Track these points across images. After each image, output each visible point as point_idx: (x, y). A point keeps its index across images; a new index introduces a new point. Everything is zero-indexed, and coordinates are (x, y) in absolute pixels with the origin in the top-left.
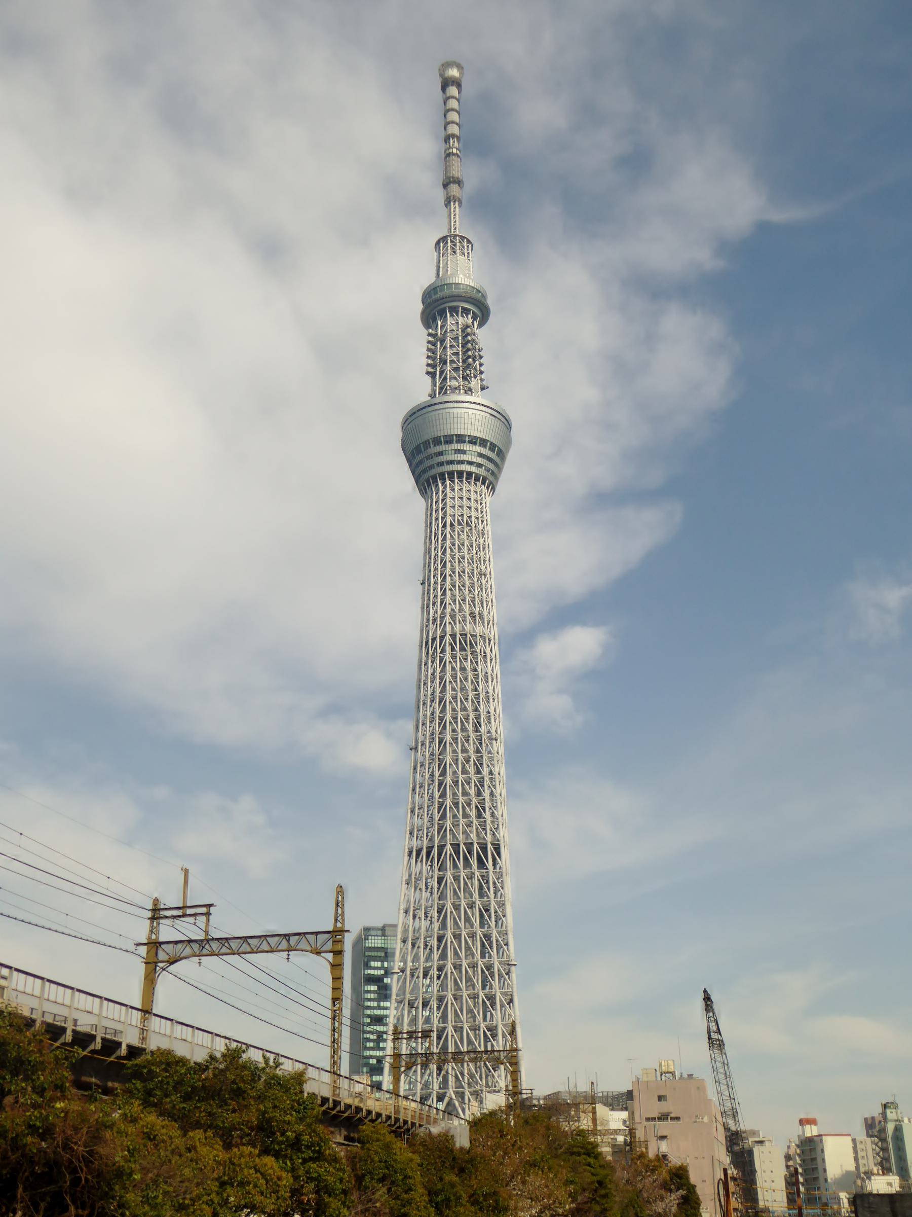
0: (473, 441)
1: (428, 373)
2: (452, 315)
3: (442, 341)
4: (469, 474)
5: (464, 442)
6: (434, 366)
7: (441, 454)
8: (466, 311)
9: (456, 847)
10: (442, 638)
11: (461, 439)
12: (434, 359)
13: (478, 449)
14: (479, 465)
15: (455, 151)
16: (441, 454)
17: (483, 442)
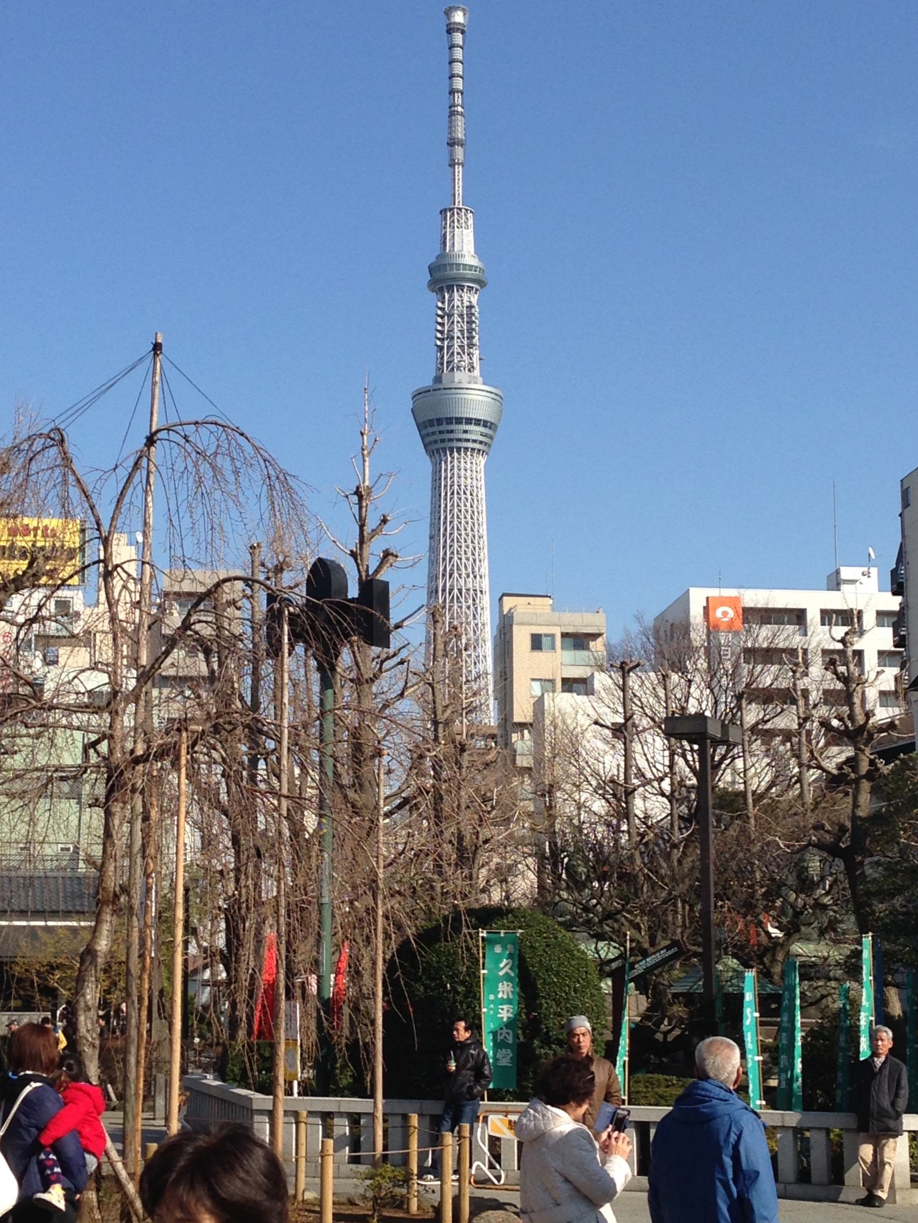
0: (478, 422)
2: (458, 291)
3: (450, 316)
4: (473, 449)
6: (442, 340)
7: (452, 431)
8: (470, 289)
10: (451, 590)
11: (469, 421)
12: (442, 332)
13: (481, 429)
14: (481, 442)
15: (460, 109)
16: (452, 431)
17: (485, 424)
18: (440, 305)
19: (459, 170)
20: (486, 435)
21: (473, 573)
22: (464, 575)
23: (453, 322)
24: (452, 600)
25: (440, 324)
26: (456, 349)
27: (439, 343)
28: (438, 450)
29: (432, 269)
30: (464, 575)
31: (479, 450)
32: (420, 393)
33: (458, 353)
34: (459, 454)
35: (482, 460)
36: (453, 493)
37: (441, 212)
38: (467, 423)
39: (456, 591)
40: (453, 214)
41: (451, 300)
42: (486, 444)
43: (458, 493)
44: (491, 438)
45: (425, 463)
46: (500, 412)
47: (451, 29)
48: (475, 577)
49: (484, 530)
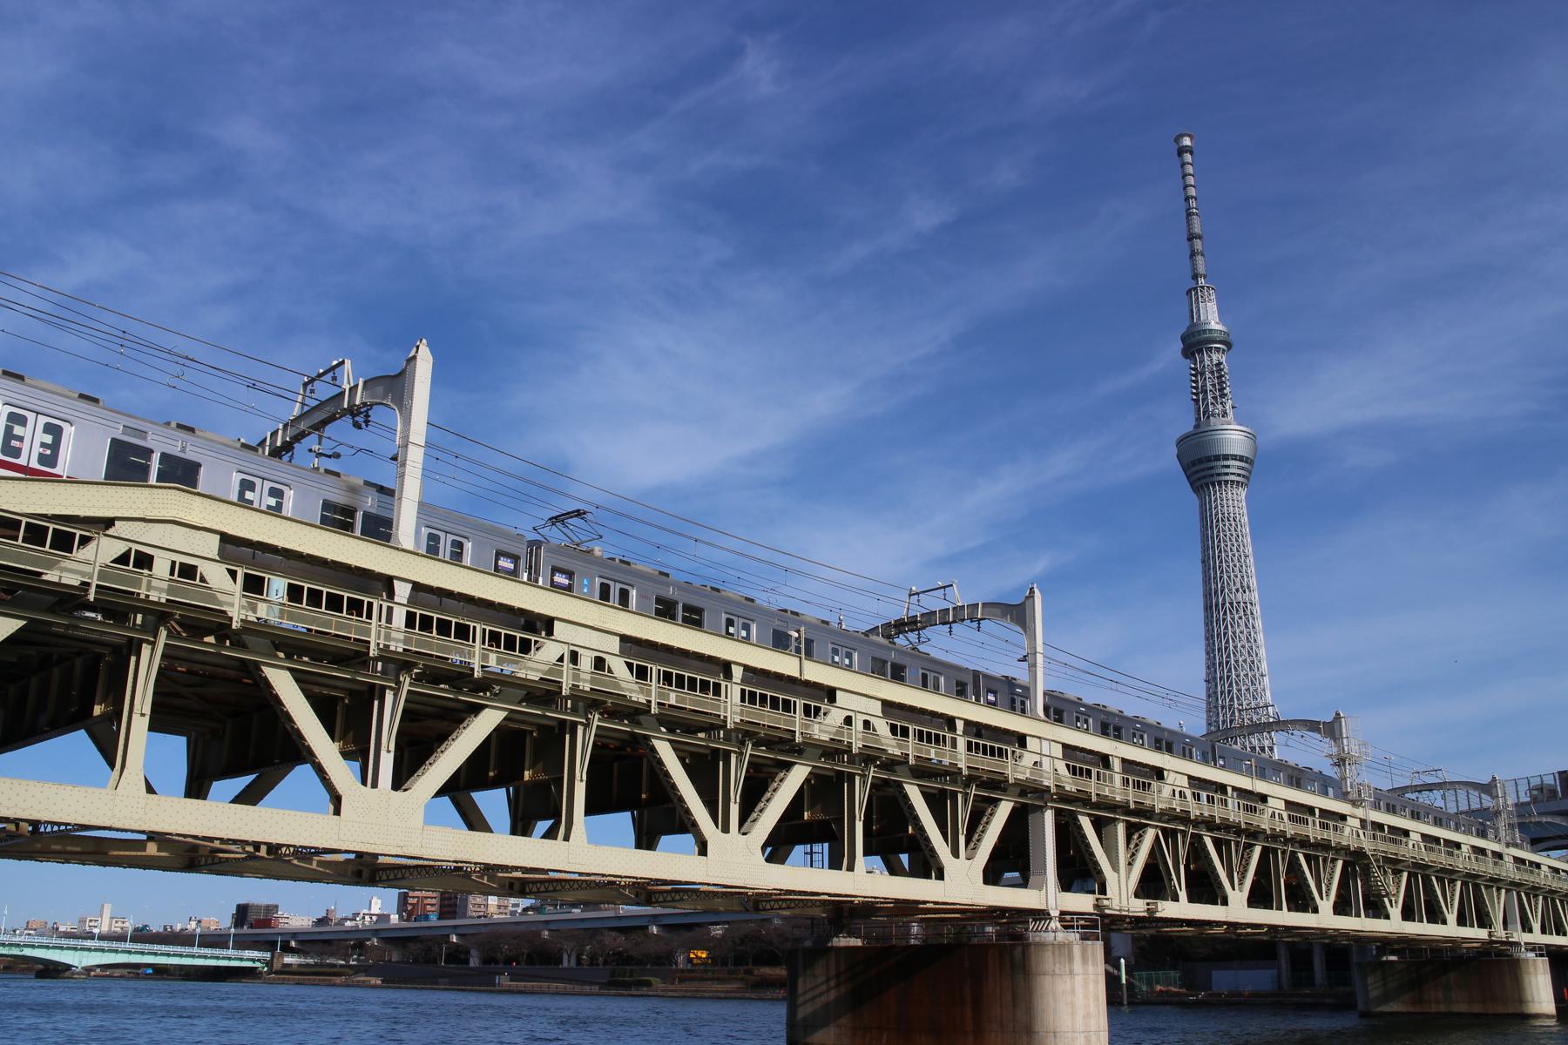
0: (1235, 457)
2: (1207, 353)
3: (1202, 374)
4: (1233, 482)
5: (1228, 459)
7: (1212, 468)
8: (1218, 349)
10: (1223, 605)
11: (1226, 457)
12: (1196, 388)
14: (1239, 475)
15: (1194, 211)
16: (1212, 468)
17: (1241, 459)
19: (1199, 258)
20: (1243, 468)
21: (1242, 587)
22: (1234, 590)
23: (1205, 379)
24: (1225, 613)
25: (1193, 381)
26: (1210, 400)
27: (1194, 397)
28: (1202, 486)
29: (1184, 339)
30: (1234, 590)
31: (1238, 482)
32: (1182, 440)
33: (1212, 403)
34: (1220, 487)
36: (1218, 521)
37: (1189, 292)
38: (1223, 460)
40: (1197, 292)
41: (1202, 361)
44: (1250, 472)
45: (1193, 499)
47: (1182, 151)
48: (1245, 592)
49: (1249, 551)
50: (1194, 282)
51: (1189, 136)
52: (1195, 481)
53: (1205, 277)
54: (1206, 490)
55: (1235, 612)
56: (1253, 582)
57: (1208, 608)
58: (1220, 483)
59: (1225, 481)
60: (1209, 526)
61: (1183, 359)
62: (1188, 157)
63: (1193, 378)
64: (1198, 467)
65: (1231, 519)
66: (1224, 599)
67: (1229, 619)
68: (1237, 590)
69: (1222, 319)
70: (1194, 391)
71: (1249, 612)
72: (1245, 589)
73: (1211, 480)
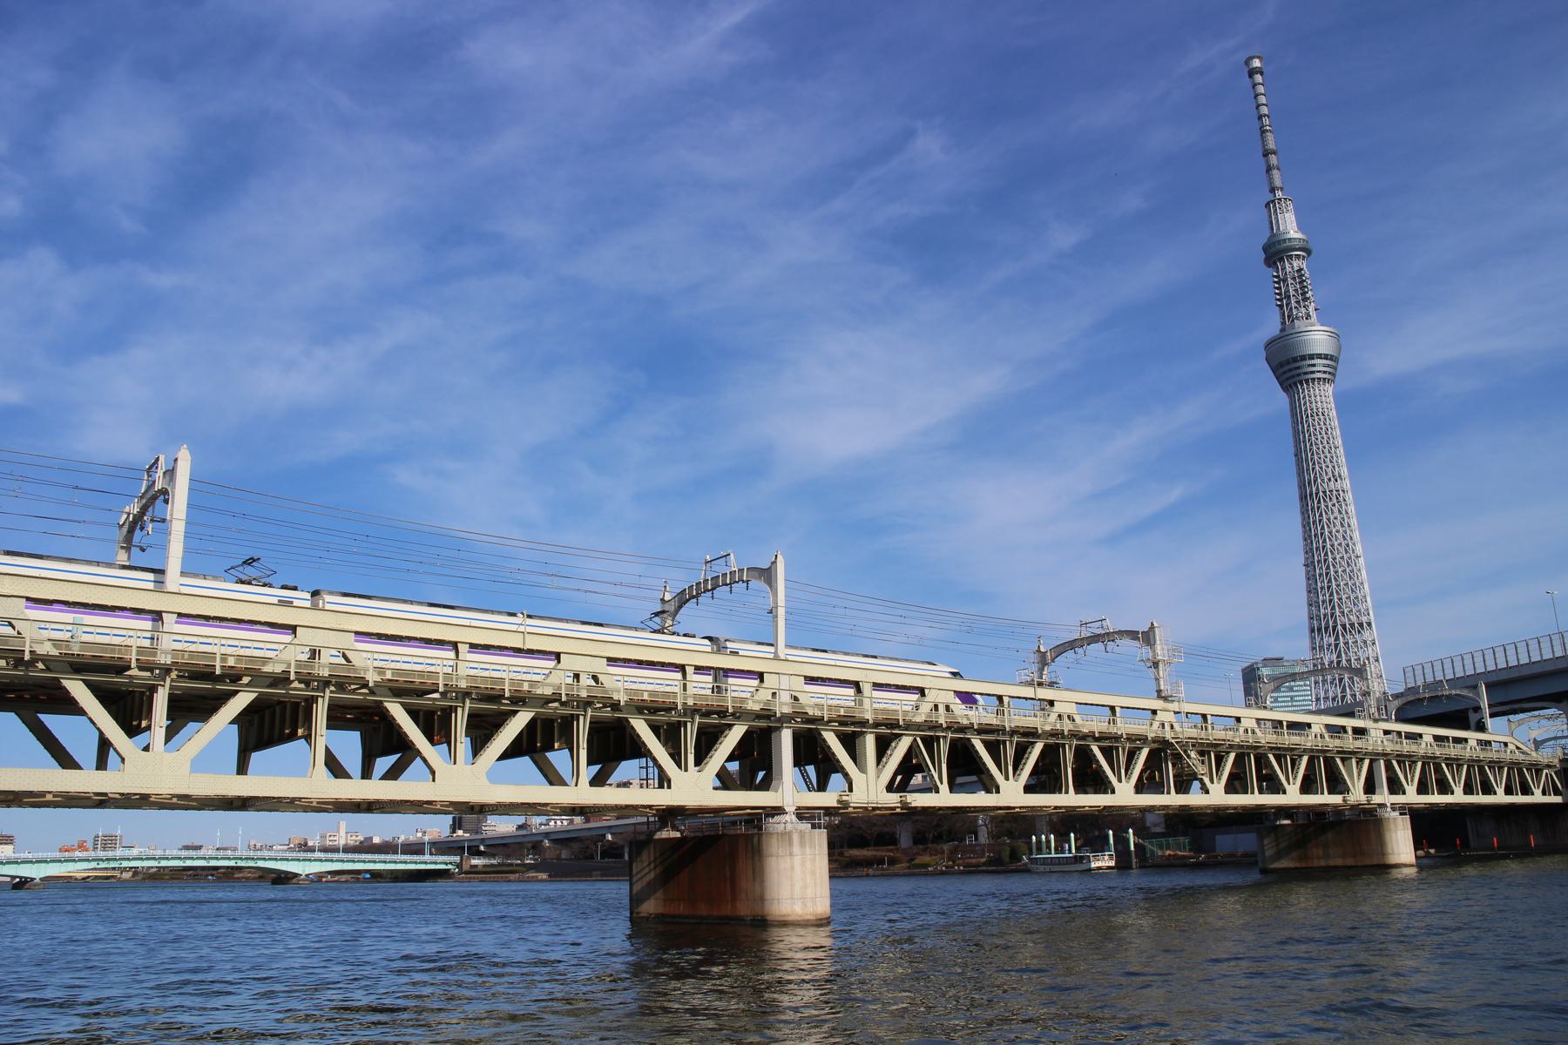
0: (1319, 356)
1: (1277, 305)
3: (1285, 280)
4: (1319, 379)
5: (1313, 359)
6: (1280, 300)
7: (1298, 368)
8: (1298, 257)
9: (1344, 626)
10: (1317, 494)
11: (1312, 357)
12: (1280, 294)
14: (1325, 372)
15: (1268, 128)
16: (1298, 368)
17: (1326, 357)
18: (1275, 274)
19: (1275, 172)
21: (1334, 476)
22: (1326, 480)
23: (1288, 285)
24: (1319, 502)
25: (1277, 288)
26: (1293, 304)
27: (1279, 303)
29: (1265, 249)
30: (1326, 480)
31: (1324, 379)
33: (1296, 307)
34: (1308, 385)
35: (1329, 389)
36: (1307, 417)
37: (1267, 205)
39: (1321, 494)
41: (1284, 269)
42: (1330, 373)
43: (1312, 416)
44: (1335, 369)
45: (1282, 398)
46: (1339, 348)
47: (1252, 73)
48: (1336, 481)
49: (1339, 441)
50: (1272, 195)
51: (1258, 57)
52: (1284, 381)
53: (1282, 189)
54: (1294, 388)
55: (1328, 500)
56: (1344, 471)
57: (1303, 498)
58: (1307, 381)
59: (1312, 379)
60: (1299, 420)
61: (1265, 267)
62: (1258, 78)
63: (1277, 285)
64: (1287, 368)
65: (1320, 414)
66: (1317, 489)
67: (1323, 506)
68: (1330, 480)
69: (1300, 228)
70: (1278, 297)
71: (1341, 499)
72: (1337, 478)
73: (1297, 378)
